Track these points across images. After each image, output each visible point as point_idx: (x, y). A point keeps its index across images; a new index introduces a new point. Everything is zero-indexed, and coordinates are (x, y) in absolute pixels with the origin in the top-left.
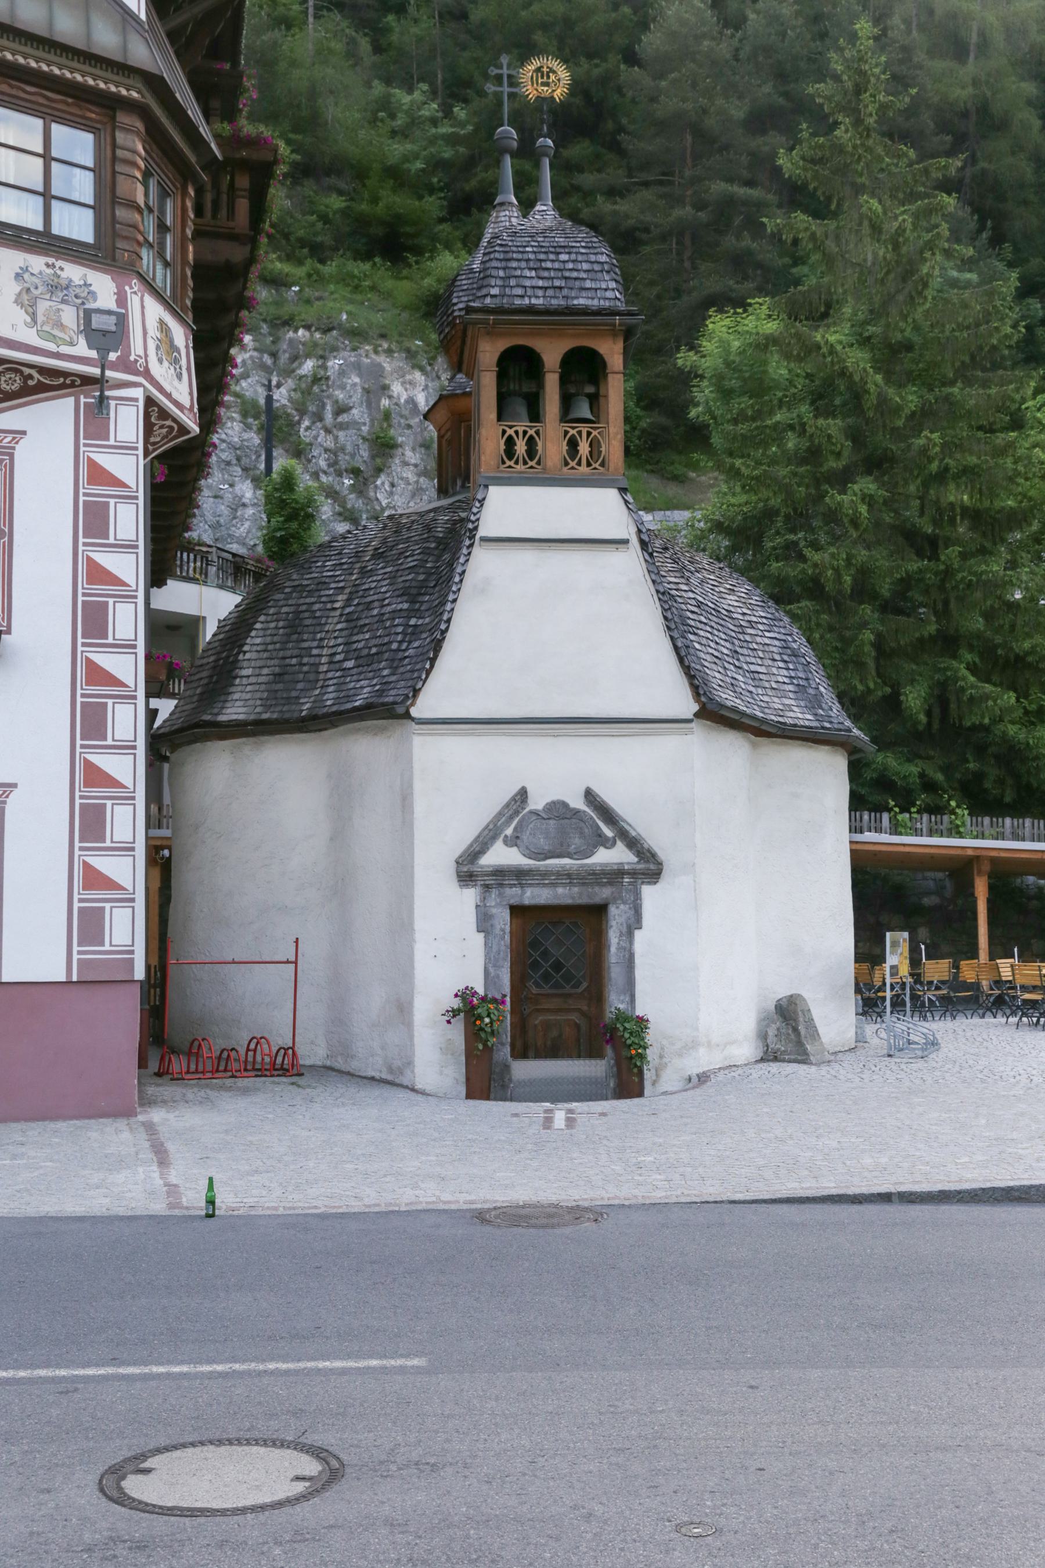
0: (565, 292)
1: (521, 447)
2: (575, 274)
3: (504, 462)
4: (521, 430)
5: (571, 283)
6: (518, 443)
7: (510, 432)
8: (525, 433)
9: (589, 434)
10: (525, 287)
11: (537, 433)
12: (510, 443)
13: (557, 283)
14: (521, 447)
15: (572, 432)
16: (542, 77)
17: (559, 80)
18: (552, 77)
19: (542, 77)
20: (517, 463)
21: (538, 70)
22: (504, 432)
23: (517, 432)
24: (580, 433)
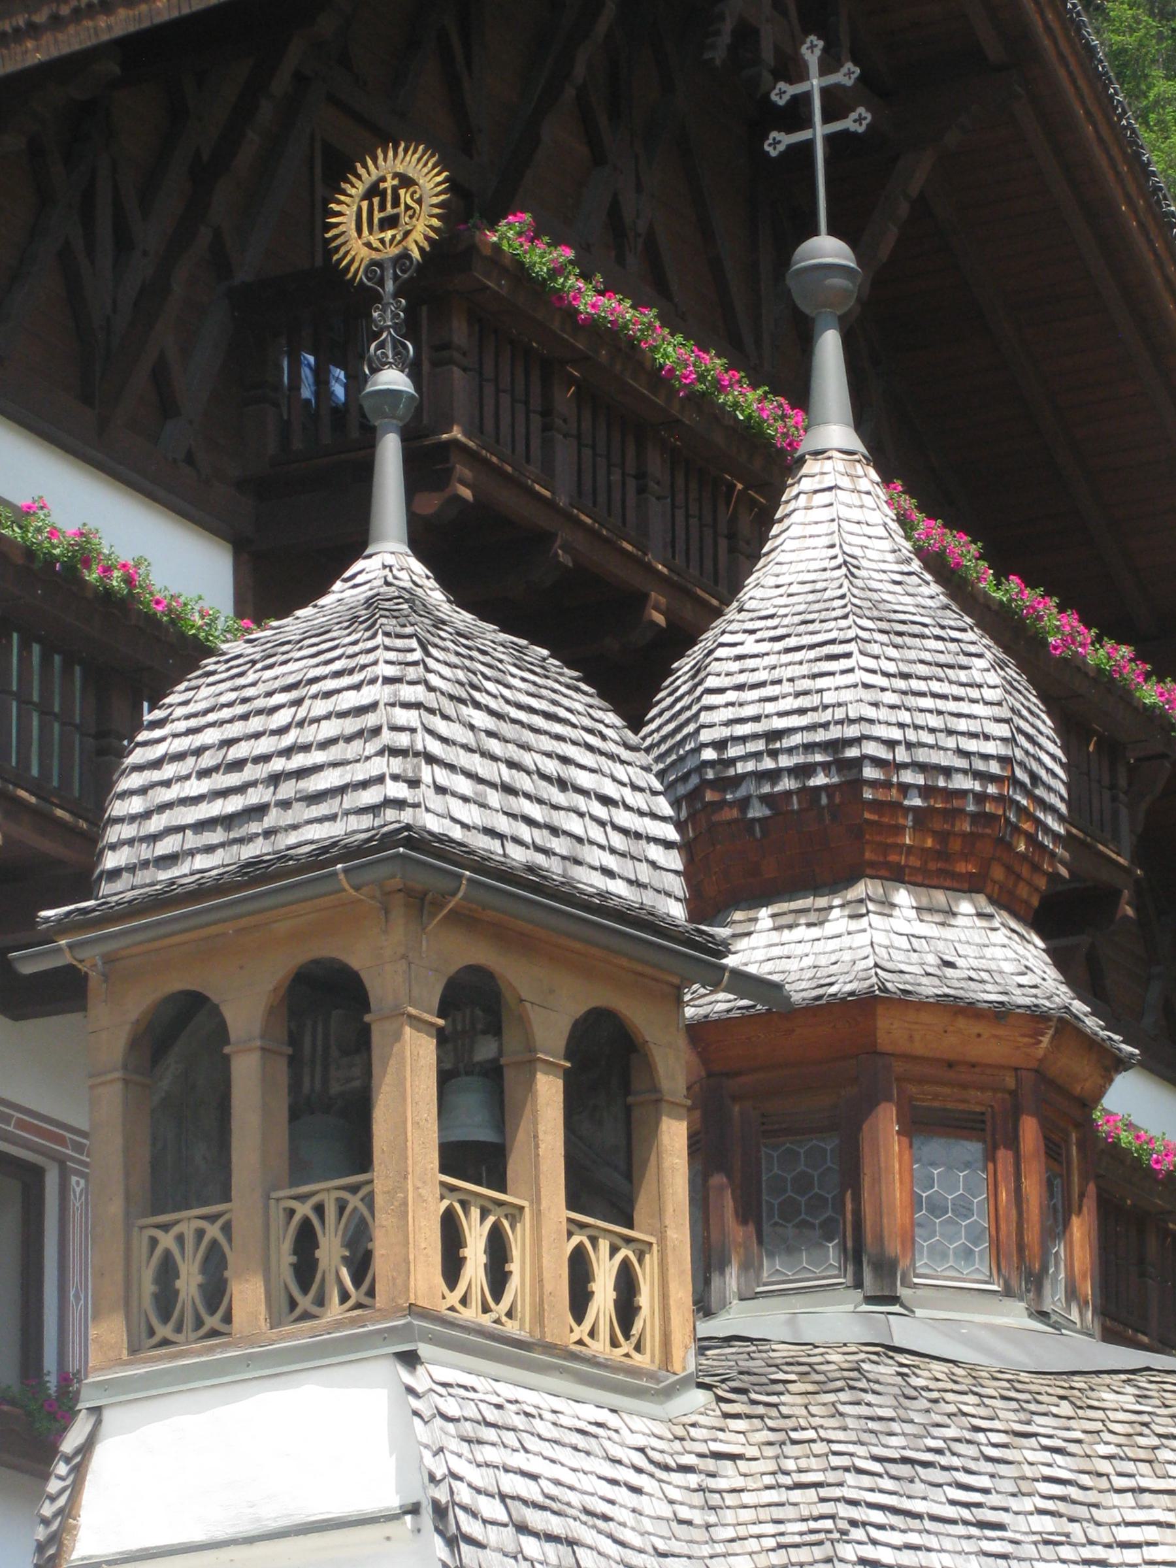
0: (273, 818)
1: (189, 1282)
2: (299, 761)
3: (152, 1333)
4: (188, 1229)
5: (287, 790)
6: (183, 1268)
7: (167, 1241)
8: (200, 1233)
9: (342, 1207)
10: (180, 829)
11: (227, 1229)
12: (167, 1271)
13: (254, 797)
14: (189, 1282)
15: (304, 1210)
16: (382, 208)
17: (419, 202)
18: (405, 196)
19: (382, 208)
20: (179, 1329)
21: (374, 191)
22: (154, 1242)
23: (180, 1239)
24: (319, 1209)
